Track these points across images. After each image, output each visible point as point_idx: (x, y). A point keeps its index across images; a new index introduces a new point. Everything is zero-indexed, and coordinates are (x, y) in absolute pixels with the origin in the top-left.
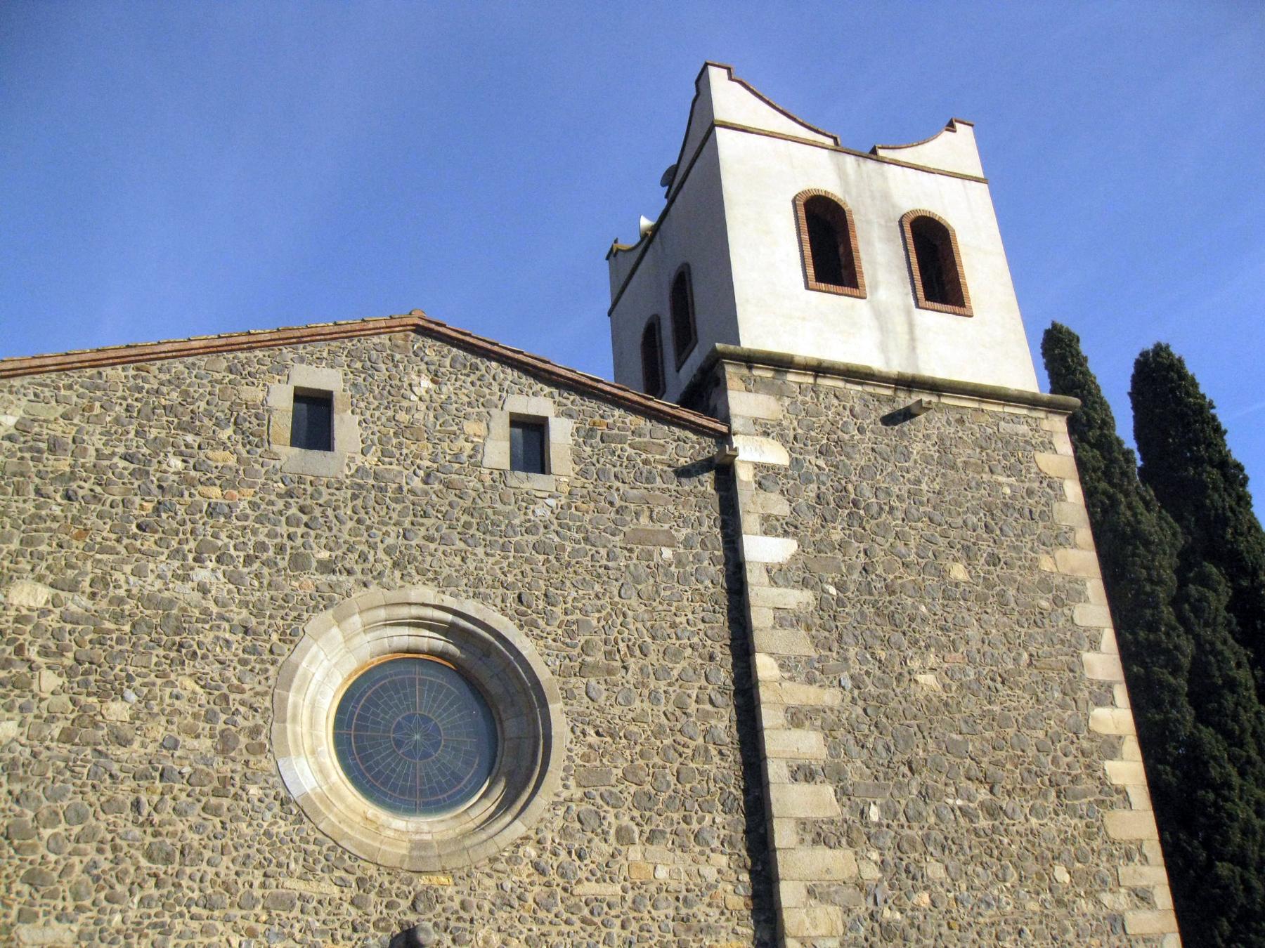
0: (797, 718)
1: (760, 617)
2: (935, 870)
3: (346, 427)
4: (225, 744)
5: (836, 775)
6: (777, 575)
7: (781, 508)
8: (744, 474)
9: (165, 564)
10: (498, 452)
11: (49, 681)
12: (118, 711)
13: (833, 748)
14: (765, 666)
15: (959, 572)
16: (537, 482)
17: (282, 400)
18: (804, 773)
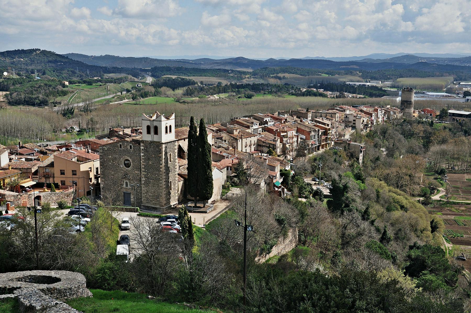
0: (143, 165)
1: (141, 159)
2: (149, 174)
3: (122, 147)
4: (118, 164)
5: (145, 168)
6: (143, 156)
7: (143, 152)
8: (141, 149)
9: (115, 155)
10: (129, 148)
11: (111, 161)
12: (114, 163)
13: (145, 167)
14: (141, 162)
15: (153, 156)
16: (131, 150)
17: (119, 145)
18: (143, 168)
